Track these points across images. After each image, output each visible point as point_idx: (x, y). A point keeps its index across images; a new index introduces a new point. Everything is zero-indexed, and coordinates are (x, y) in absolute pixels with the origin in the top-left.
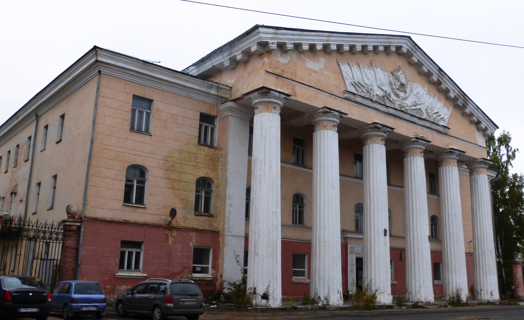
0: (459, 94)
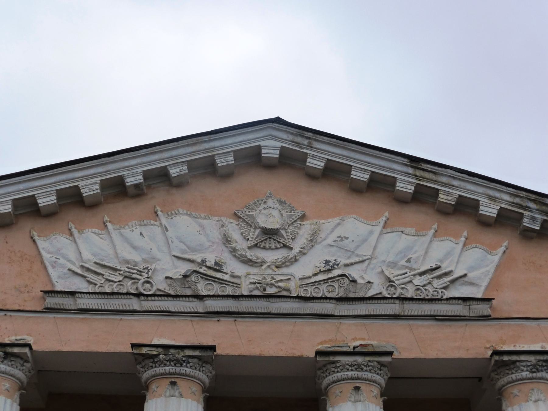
0: (517, 200)
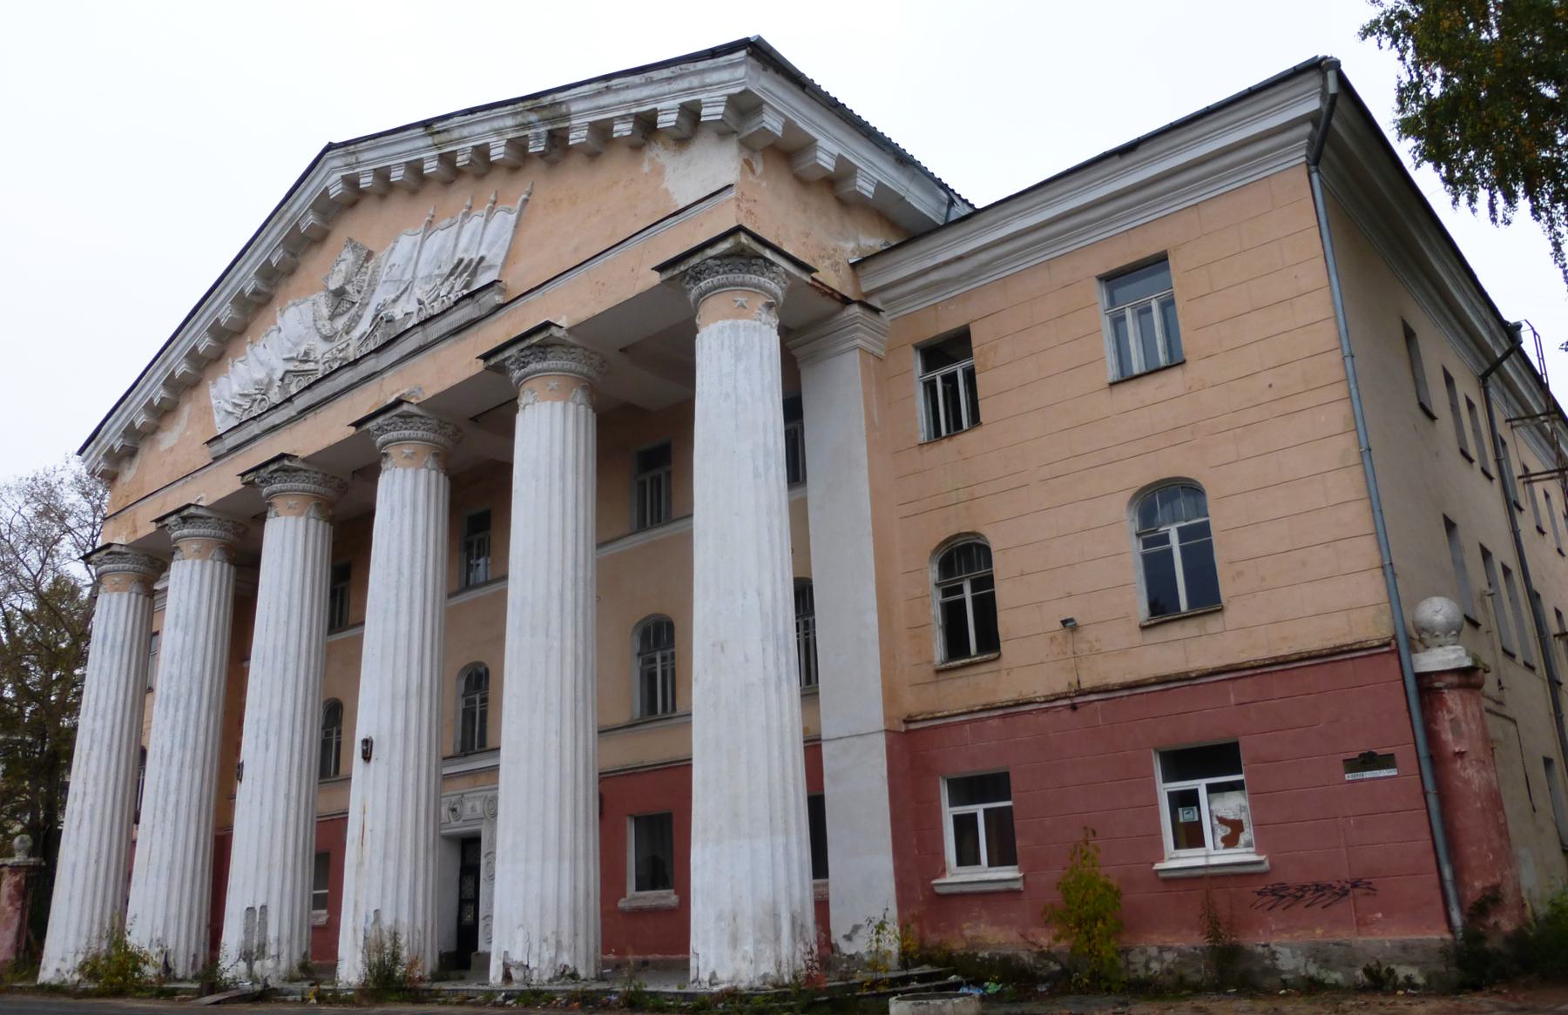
0: (519, 119)
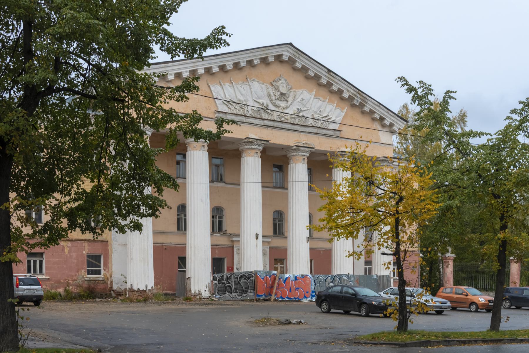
0: (355, 93)
